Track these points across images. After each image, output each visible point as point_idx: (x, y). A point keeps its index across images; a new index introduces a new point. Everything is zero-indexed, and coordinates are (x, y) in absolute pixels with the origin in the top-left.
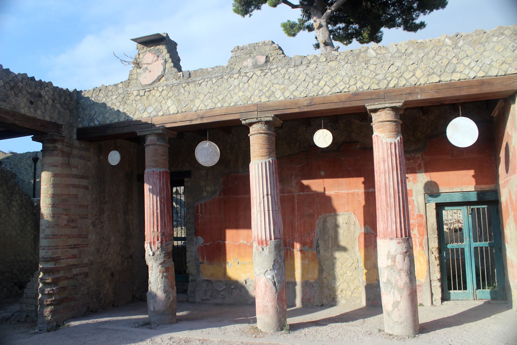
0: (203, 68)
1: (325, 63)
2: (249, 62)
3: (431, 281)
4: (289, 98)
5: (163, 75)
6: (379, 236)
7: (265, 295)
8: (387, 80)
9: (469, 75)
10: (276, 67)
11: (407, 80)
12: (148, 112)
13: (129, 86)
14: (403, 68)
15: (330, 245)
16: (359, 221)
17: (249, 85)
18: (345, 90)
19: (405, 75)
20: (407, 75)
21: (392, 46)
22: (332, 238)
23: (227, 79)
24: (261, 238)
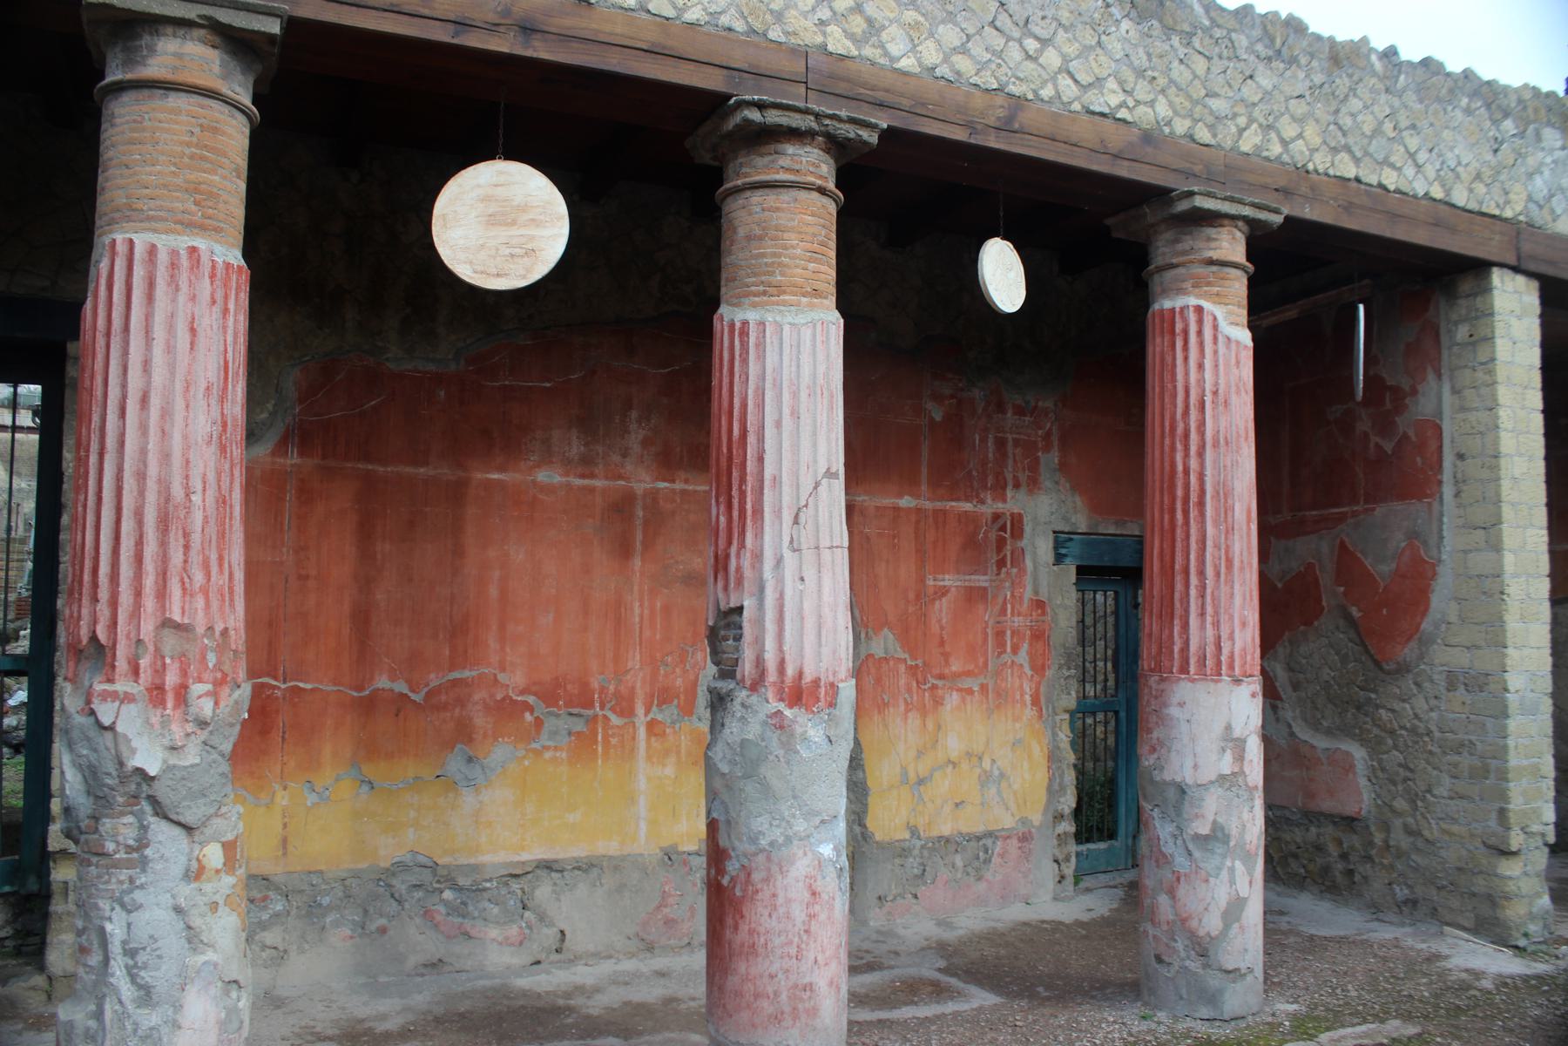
6: (1184, 669)
7: (805, 938)
8: (1237, 126)
11: (1285, 143)
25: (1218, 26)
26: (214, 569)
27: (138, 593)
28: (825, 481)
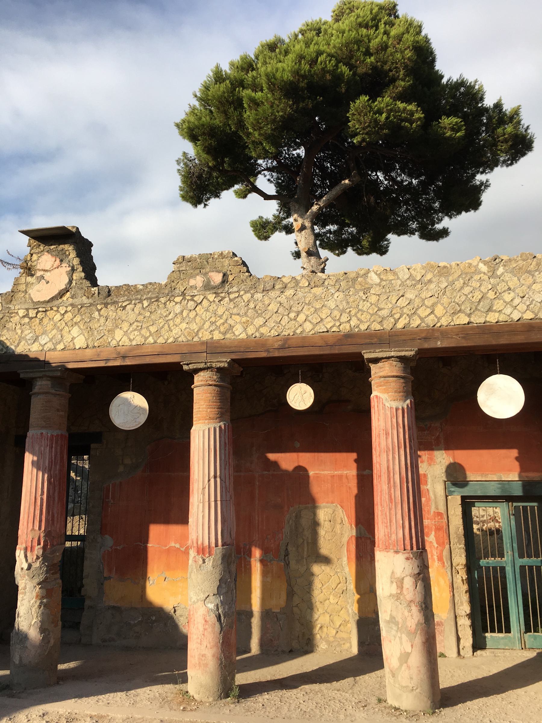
0: (130, 285)
1: (307, 290)
2: (198, 281)
3: (456, 617)
4: (254, 336)
5: (68, 289)
6: (378, 547)
8: (394, 318)
9: (512, 316)
10: (236, 291)
11: (422, 319)
12: (40, 344)
13: (13, 302)
14: (417, 302)
15: (305, 553)
16: (348, 518)
17: (197, 315)
18: (334, 329)
19: (420, 312)
20: (423, 312)
21: (403, 270)
22: (308, 543)
23: (165, 304)
24: (203, 544)
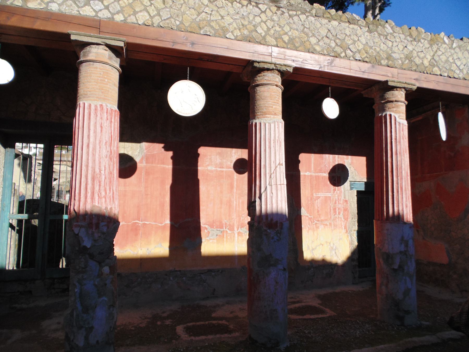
25: (395, 32)
26: (108, 192)
27: (86, 198)
28: (278, 166)
